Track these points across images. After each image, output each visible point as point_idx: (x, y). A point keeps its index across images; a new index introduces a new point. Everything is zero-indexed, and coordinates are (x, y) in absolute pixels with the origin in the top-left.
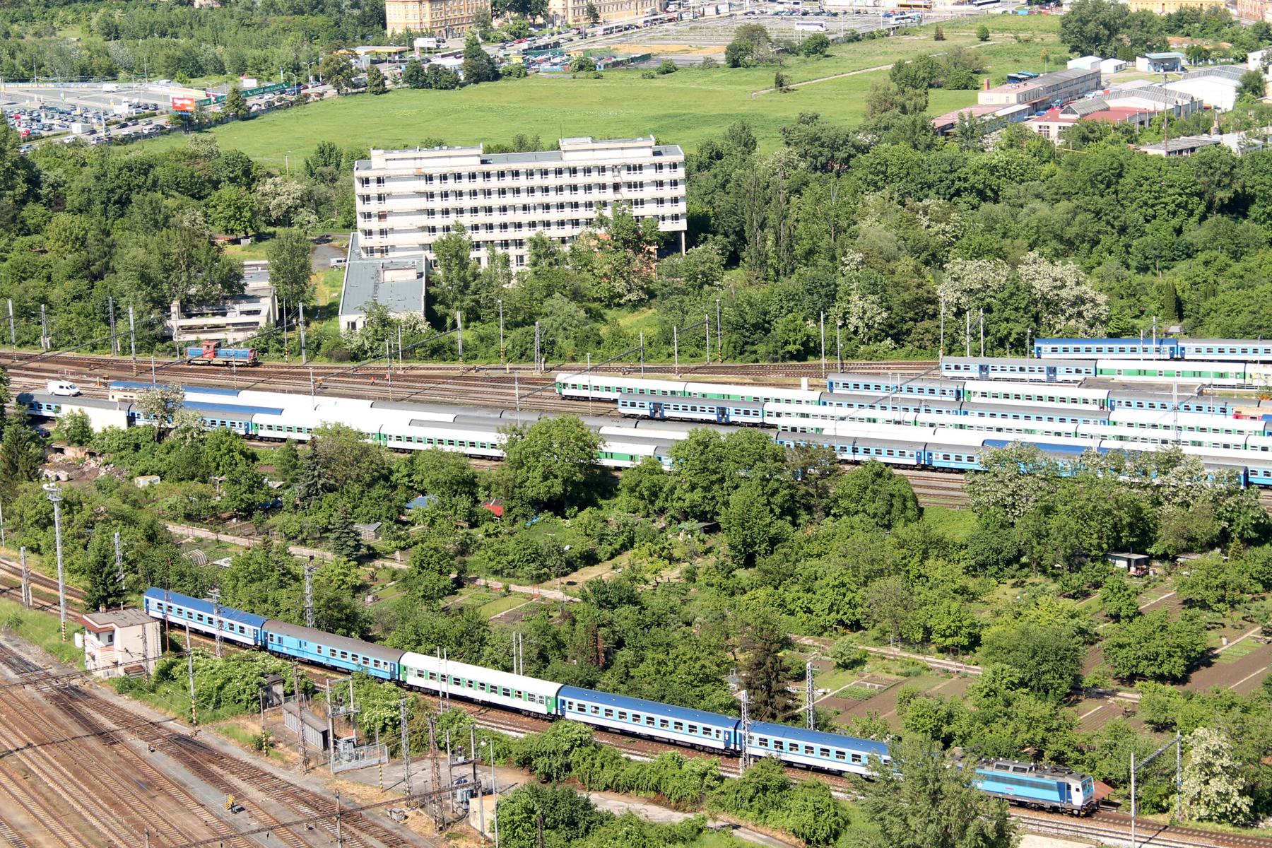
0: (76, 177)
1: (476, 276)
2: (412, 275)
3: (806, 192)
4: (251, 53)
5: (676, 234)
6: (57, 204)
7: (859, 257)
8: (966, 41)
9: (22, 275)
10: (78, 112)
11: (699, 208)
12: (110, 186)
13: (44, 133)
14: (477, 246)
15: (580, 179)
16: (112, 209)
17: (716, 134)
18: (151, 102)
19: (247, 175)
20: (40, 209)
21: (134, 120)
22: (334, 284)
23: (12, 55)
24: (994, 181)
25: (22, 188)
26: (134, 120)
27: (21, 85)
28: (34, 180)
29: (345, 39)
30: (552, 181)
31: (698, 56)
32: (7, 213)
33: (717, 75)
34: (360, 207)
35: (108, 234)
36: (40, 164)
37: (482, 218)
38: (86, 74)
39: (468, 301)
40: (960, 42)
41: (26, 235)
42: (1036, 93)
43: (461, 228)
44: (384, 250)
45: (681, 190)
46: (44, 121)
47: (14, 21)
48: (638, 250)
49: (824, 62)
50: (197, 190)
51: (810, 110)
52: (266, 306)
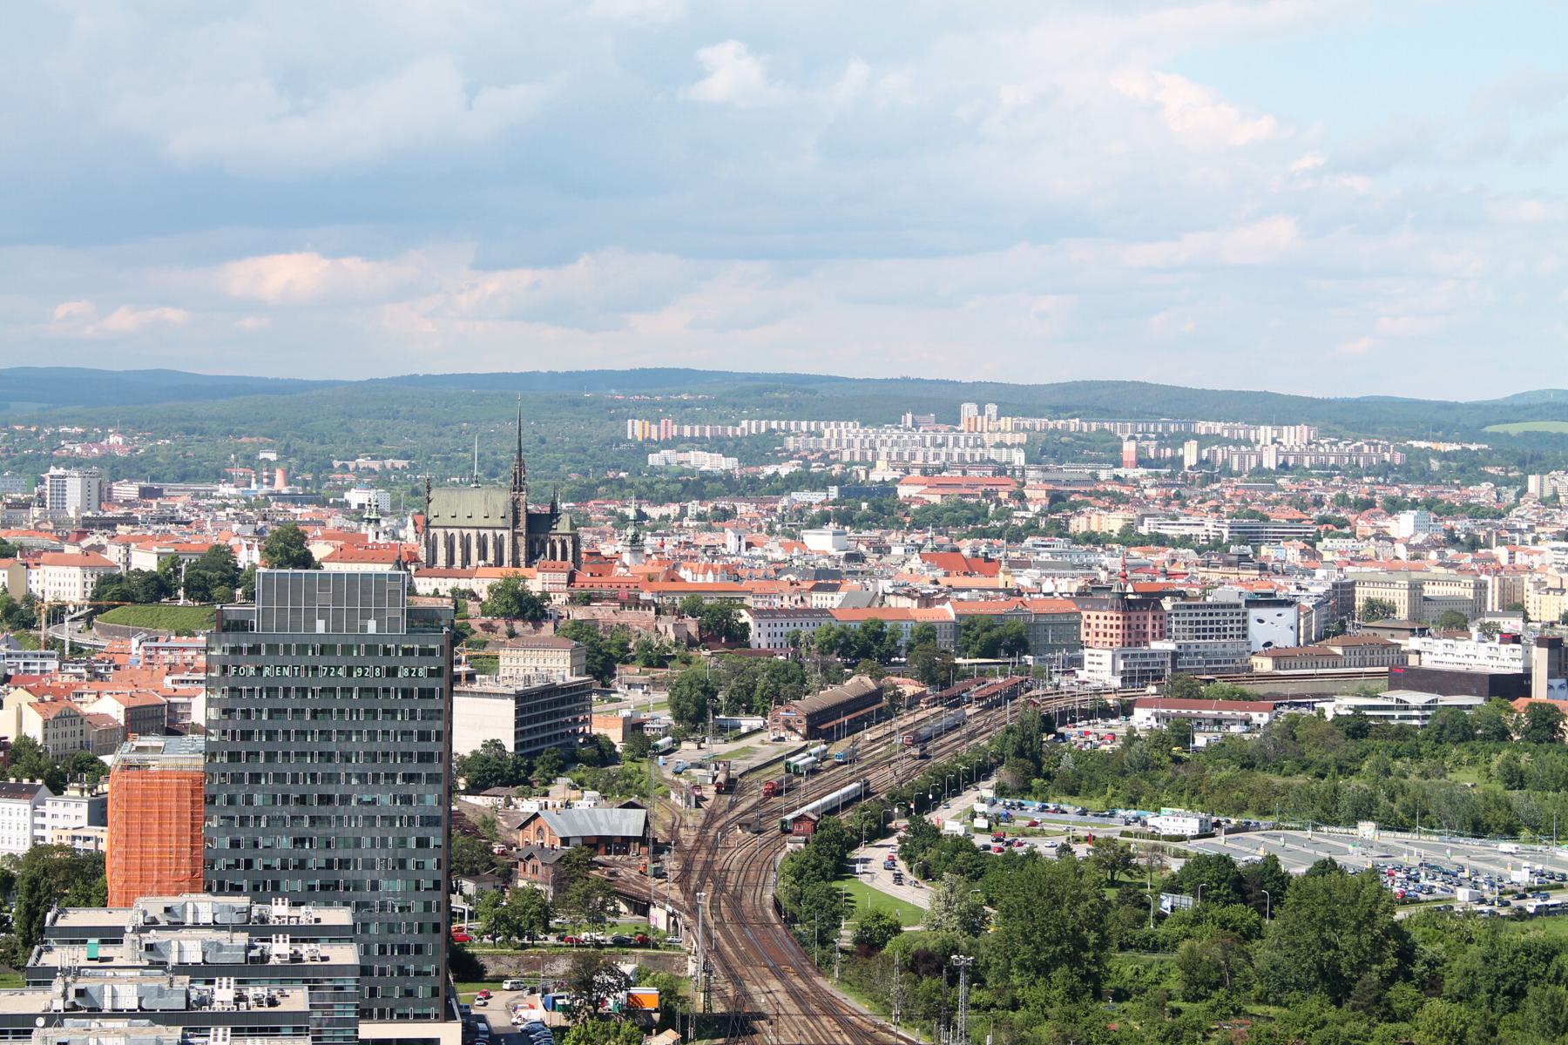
0: (1459, 956)
6: (1432, 986)
10: (1466, 874)
12: (1500, 971)
13: (1422, 897)
16: (1501, 1000)
18: (1558, 870)
20: (1411, 991)
21: (1532, 890)
23: (1392, 798)
25: (1391, 963)
27: (1399, 834)
28: (1407, 954)
32: (1370, 991)
35: (1494, 1032)
36: (1416, 935)
38: (1479, 829)
41: (1390, 1021)
46: (1423, 881)
47: (1396, 756)
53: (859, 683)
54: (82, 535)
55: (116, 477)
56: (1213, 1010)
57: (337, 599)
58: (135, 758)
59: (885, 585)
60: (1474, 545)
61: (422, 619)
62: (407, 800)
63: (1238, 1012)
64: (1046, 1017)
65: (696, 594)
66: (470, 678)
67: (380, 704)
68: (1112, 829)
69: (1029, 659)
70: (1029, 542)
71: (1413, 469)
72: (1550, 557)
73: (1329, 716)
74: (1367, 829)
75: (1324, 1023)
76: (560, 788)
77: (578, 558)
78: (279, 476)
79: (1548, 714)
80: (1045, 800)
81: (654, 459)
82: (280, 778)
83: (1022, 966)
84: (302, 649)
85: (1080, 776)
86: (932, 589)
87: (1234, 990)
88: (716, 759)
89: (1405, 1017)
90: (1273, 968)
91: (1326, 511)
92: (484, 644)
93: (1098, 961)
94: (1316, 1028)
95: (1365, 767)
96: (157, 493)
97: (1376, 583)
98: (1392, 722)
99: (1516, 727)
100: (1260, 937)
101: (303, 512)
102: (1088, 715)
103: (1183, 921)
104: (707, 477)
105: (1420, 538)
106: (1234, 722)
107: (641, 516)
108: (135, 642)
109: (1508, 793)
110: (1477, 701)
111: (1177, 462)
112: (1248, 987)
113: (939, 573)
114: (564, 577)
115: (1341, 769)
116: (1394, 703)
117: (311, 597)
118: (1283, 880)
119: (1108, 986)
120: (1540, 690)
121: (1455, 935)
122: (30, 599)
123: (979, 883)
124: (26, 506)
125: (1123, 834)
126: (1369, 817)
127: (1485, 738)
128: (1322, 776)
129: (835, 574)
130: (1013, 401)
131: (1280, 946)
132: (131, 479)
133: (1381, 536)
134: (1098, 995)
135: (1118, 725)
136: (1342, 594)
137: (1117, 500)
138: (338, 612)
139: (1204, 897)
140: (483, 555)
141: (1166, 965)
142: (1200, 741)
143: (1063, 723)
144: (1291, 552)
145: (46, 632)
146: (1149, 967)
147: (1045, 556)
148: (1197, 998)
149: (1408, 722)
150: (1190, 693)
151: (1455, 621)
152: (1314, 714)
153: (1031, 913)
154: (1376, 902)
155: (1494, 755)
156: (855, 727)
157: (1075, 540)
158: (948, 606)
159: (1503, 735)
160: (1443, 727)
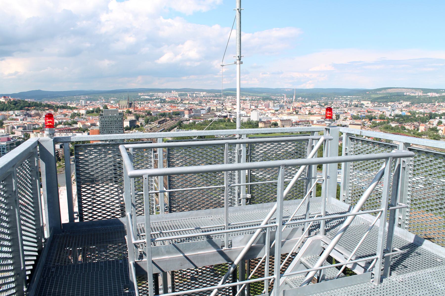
53: (163, 118)
54: (84, 107)
55: (87, 101)
57: (112, 112)
58: (92, 129)
59: (165, 109)
61: (120, 114)
62: (120, 132)
65: (147, 110)
66: (124, 119)
67: (116, 122)
69: (180, 116)
70: (179, 104)
71: (216, 96)
72: (229, 104)
76: (134, 130)
77: (135, 107)
78: (104, 100)
81: (141, 97)
82: (107, 130)
84: (108, 117)
86: (170, 109)
88: (149, 126)
91: (208, 100)
92: (126, 116)
96: (92, 102)
97: (212, 107)
101: (106, 104)
102: (186, 121)
104: (147, 99)
105: (217, 103)
107: (141, 103)
108: (91, 117)
110: (223, 118)
111: (193, 96)
113: (170, 108)
114: (133, 109)
117: (109, 112)
120: (228, 117)
122: (80, 113)
124: (78, 104)
130: (177, 90)
132: (89, 101)
133: (213, 103)
135: (189, 122)
136: (210, 108)
137: (188, 100)
138: (112, 113)
140: (125, 107)
142: (196, 123)
144: (205, 105)
145: (81, 116)
147: (181, 106)
150: (195, 118)
151: (219, 110)
156: (163, 123)
157: (183, 104)
158: (171, 111)
159: (225, 121)
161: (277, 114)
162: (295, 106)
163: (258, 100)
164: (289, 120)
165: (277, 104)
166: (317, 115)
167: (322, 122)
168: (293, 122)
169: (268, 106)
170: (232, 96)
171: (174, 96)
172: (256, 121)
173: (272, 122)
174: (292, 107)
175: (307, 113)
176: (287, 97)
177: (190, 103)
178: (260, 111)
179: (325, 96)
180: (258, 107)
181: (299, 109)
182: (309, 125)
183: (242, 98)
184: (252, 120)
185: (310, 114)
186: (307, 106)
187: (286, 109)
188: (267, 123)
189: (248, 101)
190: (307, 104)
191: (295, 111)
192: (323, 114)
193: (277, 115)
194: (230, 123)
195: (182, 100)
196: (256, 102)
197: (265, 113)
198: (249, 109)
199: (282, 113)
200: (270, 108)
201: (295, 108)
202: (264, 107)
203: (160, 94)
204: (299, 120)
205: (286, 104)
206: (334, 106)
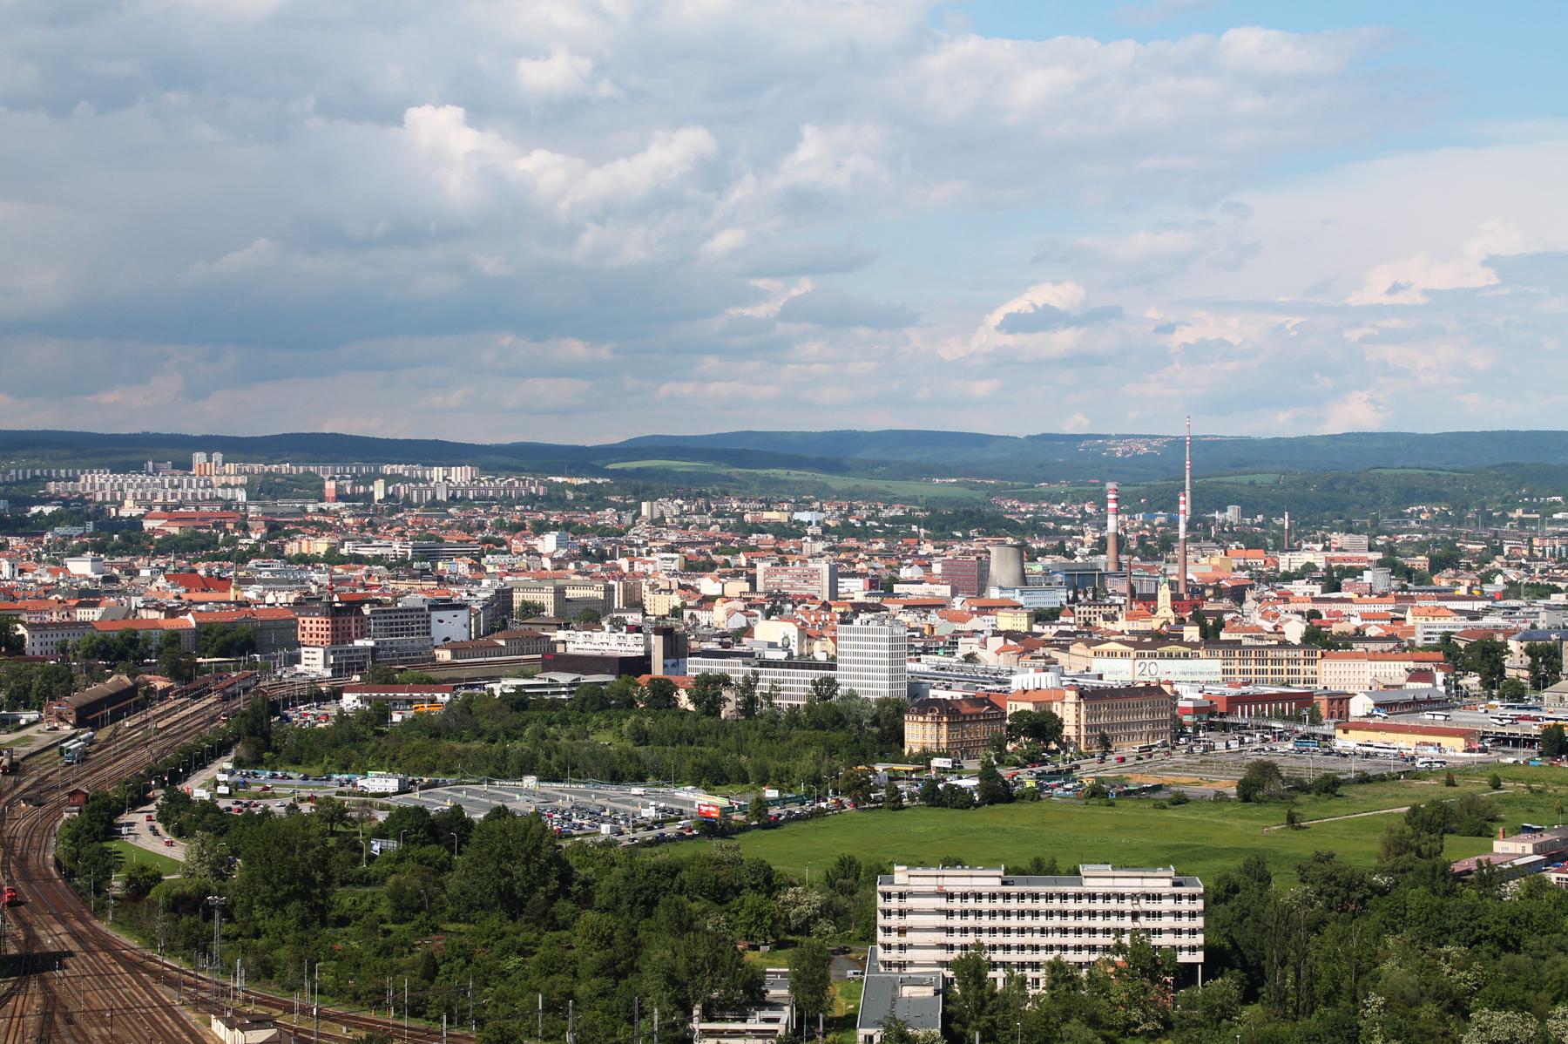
1: (993, 996)
2: (928, 992)
3: (1328, 931)
4: (773, 765)
5: (1194, 965)
6: (585, 901)
7: (1381, 1000)
8: (1478, 787)
9: (550, 969)
10: (607, 813)
11: (1217, 940)
13: (574, 832)
14: (994, 966)
15: (1099, 905)
16: (639, 909)
17: (1232, 865)
19: (769, 883)
20: (570, 906)
21: (660, 823)
22: (850, 995)
23: (549, 756)
24: (1516, 931)
26: (660, 823)
27: (554, 785)
28: (566, 876)
29: (864, 753)
30: (1071, 905)
31: (1208, 789)
32: (539, 907)
33: (1229, 809)
34: (881, 921)
35: (635, 934)
36: (573, 862)
37: (999, 939)
38: (616, 778)
39: (984, 1021)
40: (1473, 789)
41: (554, 930)
42: (1551, 843)
43: (979, 946)
44: (902, 965)
45: (1199, 922)
47: (550, 724)
48: (1154, 980)
49: (1335, 802)
50: (722, 894)
51: (1325, 848)
52: (785, 1015)
56: (416, 929)
59: (137, 601)
60: (601, 557)
63: (436, 930)
64: (284, 942)
68: (329, 789)
70: (252, 563)
71: (554, 499)
72: (660, 565)
73: (497, 694)
74: (530, 781)
75: (504, 934)
79: (664, 686)
80: (274, 769)
83: (262, 902)
85: (302, 749)
87: (432, 913)
89: (566, 926)
90: (463, 894)
91: (487, 533)
93: (324, 895)
94: (497, 939)
95: (526, 734)
98: (546, 697)
99: (640, 698)
100: (450, 869)
103: (389, 860)
105: (562, 553)
106: (422, 701)
109: (637, 749)
110: (610, 678)
111: (369, 496)
112: (443, 910)
113: (181, 590)
115: (508, 735)
116: (547, 682)
118: (468, 824)
119: (332, 915)
120: (658, 669)
121: (602, 860)
123: (224, 838)
125: (338, 793)
126: (531, 772)
127: (617, 707)
128: (493, 741)
129: (96, 593)
131: (467, 876)
133: (532, 552)
134: (324, 924)
135: (331, 709)
136: (503, 597)
137: (322, 528)
139: (405, 841)
141: (378, 896)
143: (287, 708)
144: (462, 567)
146: (364, 897)
147: (265, 575)
148: (402, 921)
149: (558, 697)
150: (388, 681)
151: (590, 615)
152: (486, 693)
153: (269, 860)
154: (541, 838)
155: (624, 720)
156: (116, 717)
160: (585, 700)
161: (1048, 643)
162: (1189, 576)
163: (890, 534)
164: (1152, 691)
165: (1048, 561)
166: (1372, 647)
167: (1416, 705)
168: (1181, 704)
169: (974, 580)
170: (687, 497)
171: (214, 500)
172: (883, 703)
173: (1011, 708)
174: (1173, 585)
175: (1295, 630)
176: (1127, 504)
177: (344, 551)
178: (909, 618)
179: (1434, 497)
180: (897, 588)
181: (1226, 602)
182: (1316, 730)
183: (767, 515)
184: (852, 695)
185: (1319, 640)
186: (1288, 577)
187: (1120, 600)
188: (975, 719)
189: (815, 538)
190: (1288, 562)
191: (1198, 618)
192: (1419, 642)
193: (1055, 654)
194: (669, 720)
195: (274, 529)
196: (881, 545)
197: (957, 634)
198: (826, 607)
199: (1088, 635)
200: (994, 594)
201: (1197, 591)
202: (944, 590)
203: (97, 483)
204: (1233, 692)
205: (1124, 558)
206: (1512, 575)
